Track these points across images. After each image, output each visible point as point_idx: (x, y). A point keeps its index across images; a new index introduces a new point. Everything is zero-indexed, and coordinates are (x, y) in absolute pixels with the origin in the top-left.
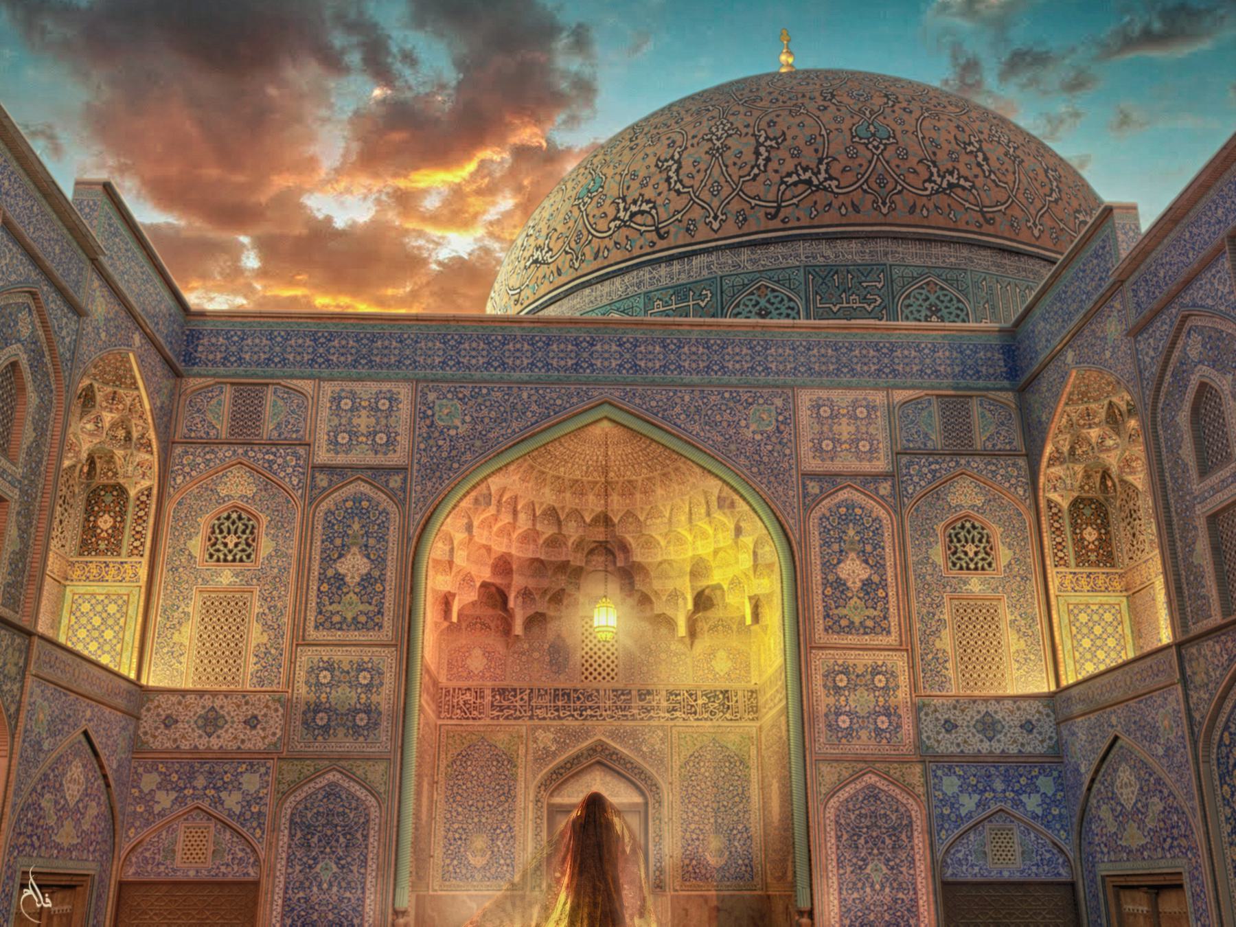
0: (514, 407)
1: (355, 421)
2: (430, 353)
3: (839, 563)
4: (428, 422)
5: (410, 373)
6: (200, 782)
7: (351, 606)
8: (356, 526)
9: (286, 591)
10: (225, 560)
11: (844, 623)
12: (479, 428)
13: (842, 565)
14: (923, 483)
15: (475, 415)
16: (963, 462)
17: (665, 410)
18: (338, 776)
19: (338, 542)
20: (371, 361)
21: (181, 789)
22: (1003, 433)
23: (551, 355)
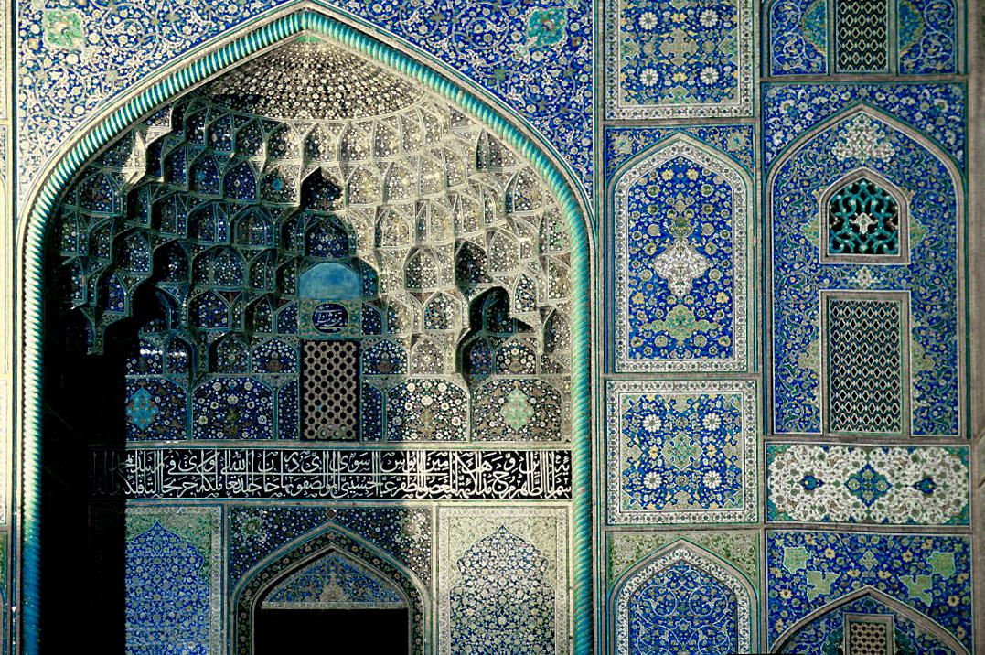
3: (658, 253)
4: (34, 44)
13: (663, 256)
14: (798, 128)
15: (105, 32)
17: (397, 19)
22: (935, 42)
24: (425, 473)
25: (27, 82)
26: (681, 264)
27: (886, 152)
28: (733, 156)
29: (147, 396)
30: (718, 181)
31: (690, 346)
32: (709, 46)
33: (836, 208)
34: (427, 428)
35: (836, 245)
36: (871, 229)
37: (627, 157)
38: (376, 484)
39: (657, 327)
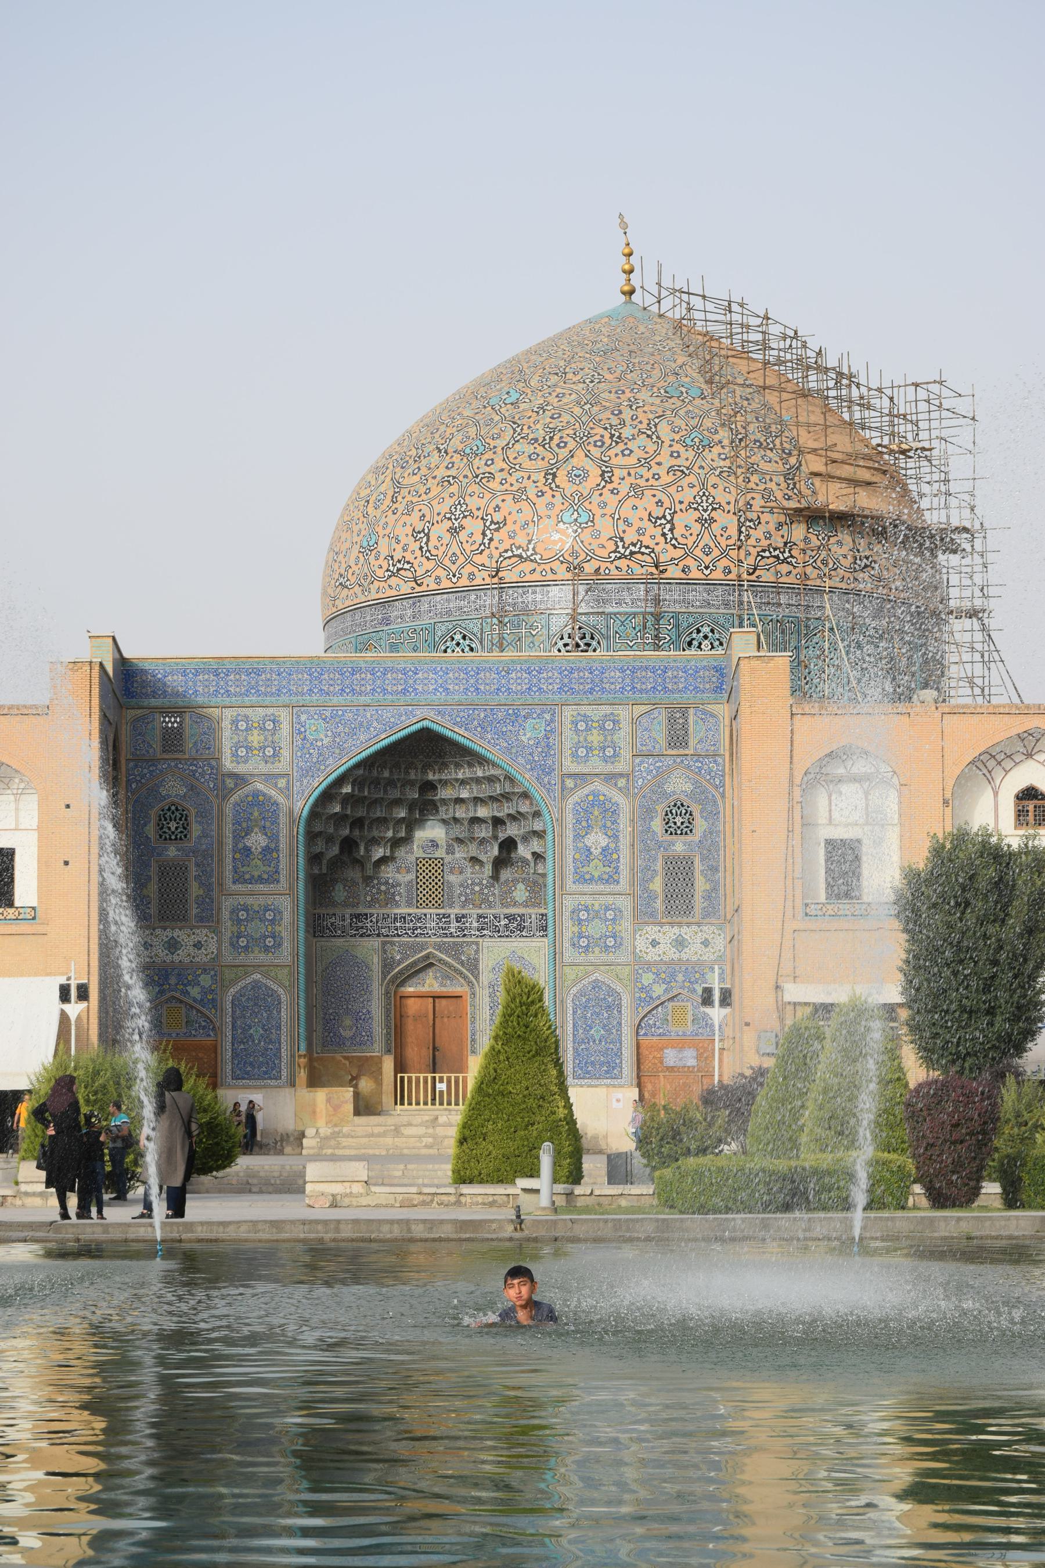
0: (361, 724)
1: (250, 738)
2: (300, 683)
5: (284, 699)
6: (173, 981)
7: (258, 867)
8: (256, 814)
9: (212, 860)
10: (170, 839)
11: (587, 877)
12: (338, 740)
14: (649, 777)
16: (678, 760)
18: (259, 976)
19: (244, 825)
20: (258, 691)
21: (162, 985)
23: (387, 682)
24: (475, 925)
25: (299, 754)
26: (597, 840)
27: (688, 787)
28: (620, 789)
29: (342, 887)
30: (613, 801)
31: (600, 879)
32: (609, 738)
33: (667, 815)
34: (478, 902)
35: (667, 831)
36: (682, 823)
37: (572, 789)
38: (453, 930)
39: (585, 869)
